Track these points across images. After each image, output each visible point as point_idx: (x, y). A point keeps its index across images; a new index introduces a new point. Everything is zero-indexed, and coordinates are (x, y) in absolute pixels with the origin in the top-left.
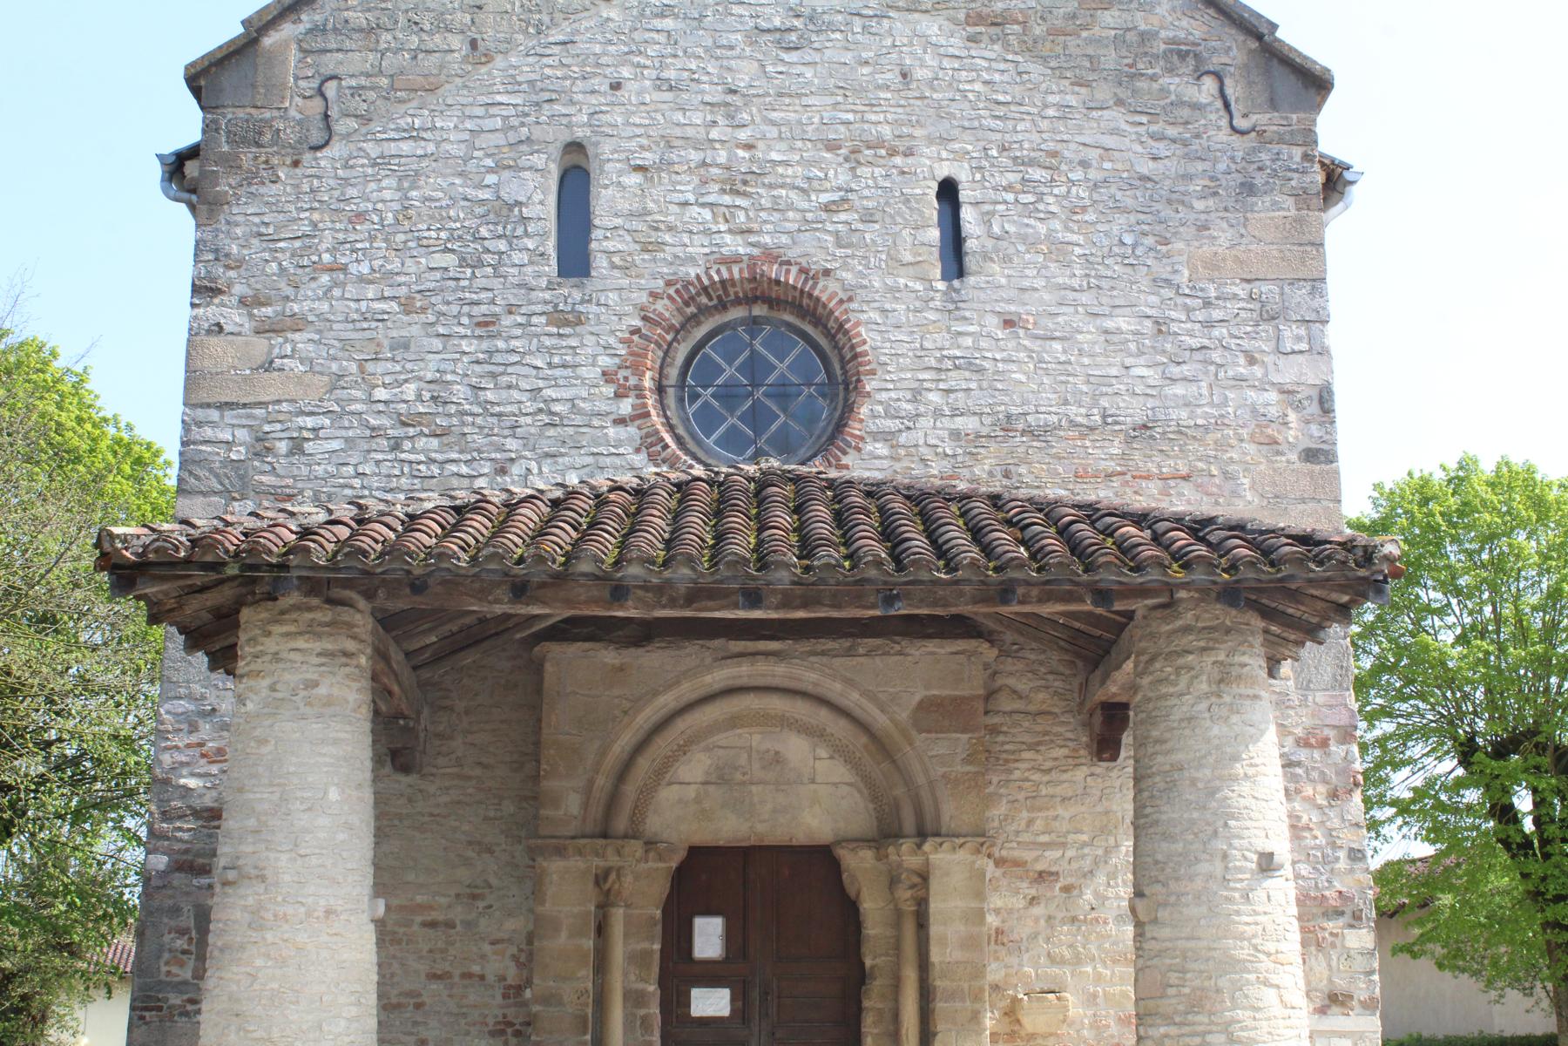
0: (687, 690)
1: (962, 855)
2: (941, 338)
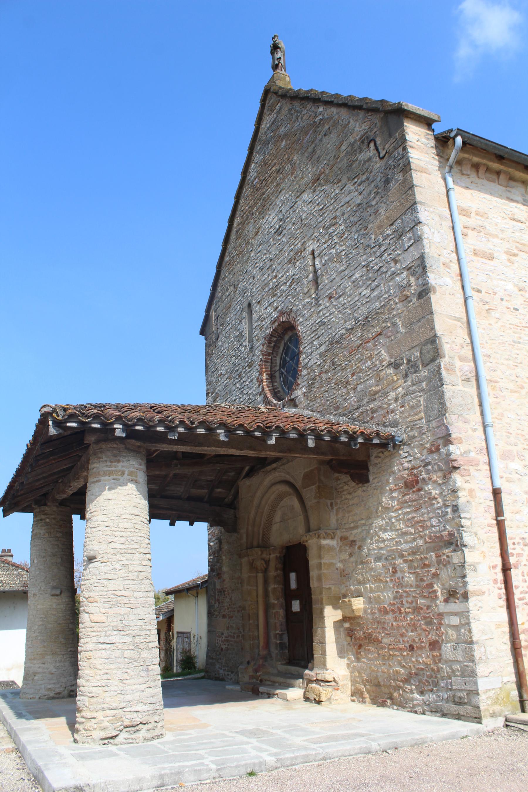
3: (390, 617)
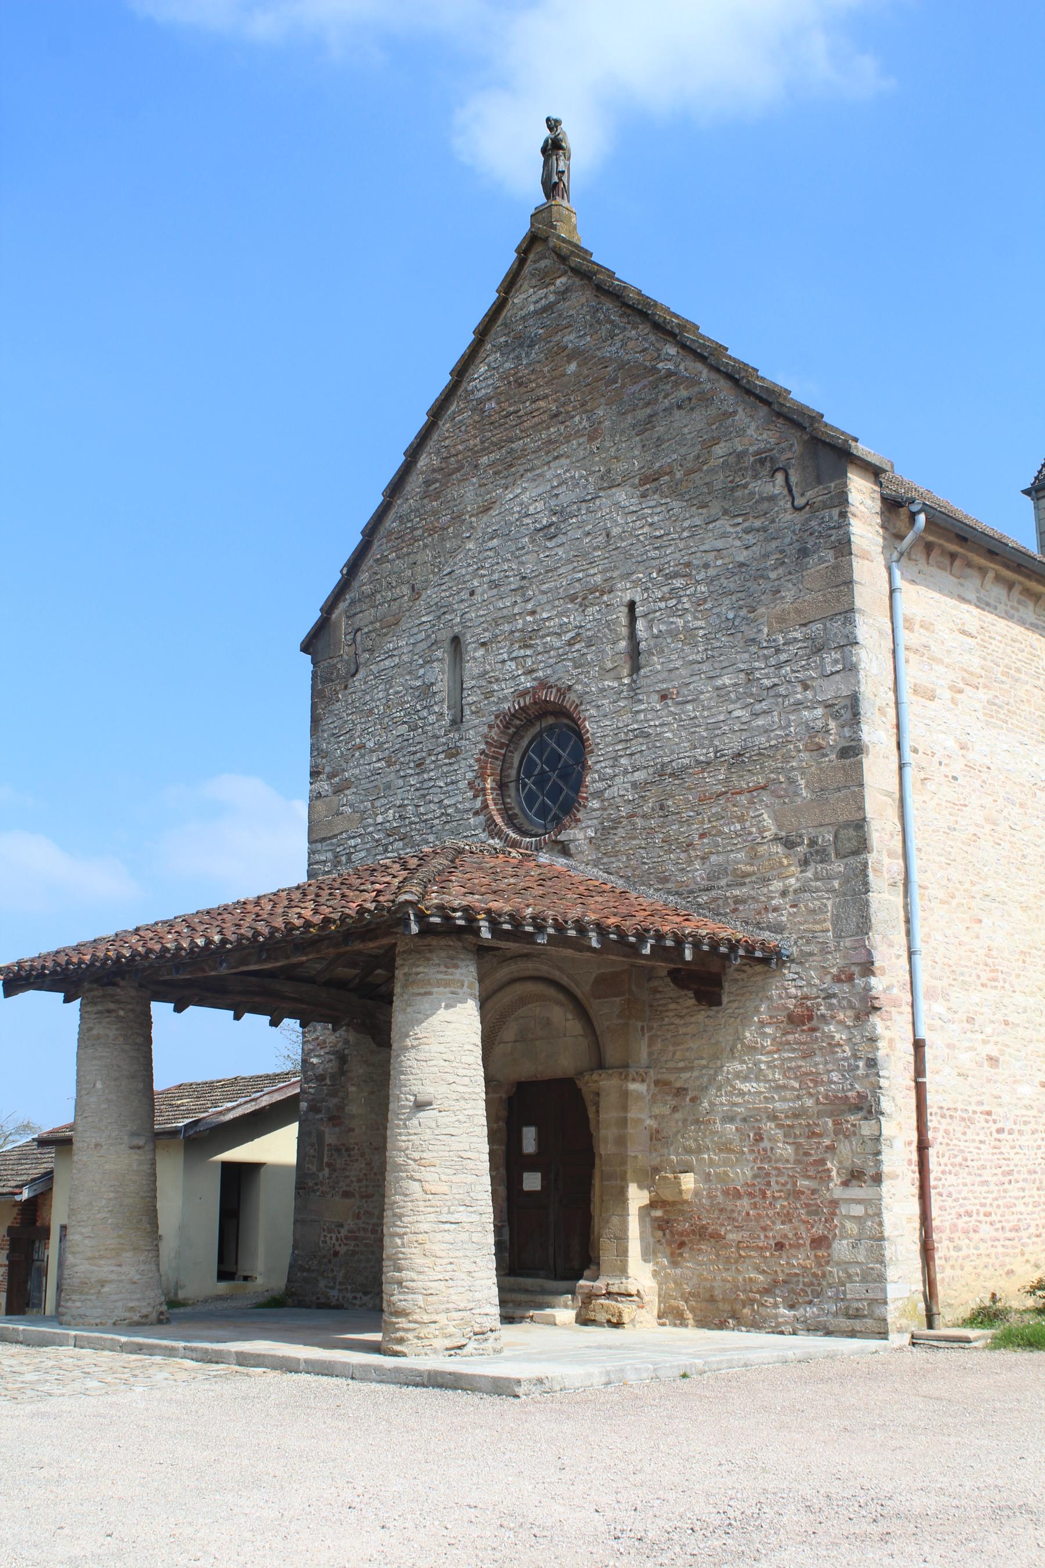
1: (615, 1082)
2: (627, 718)
3: (745, 1202)
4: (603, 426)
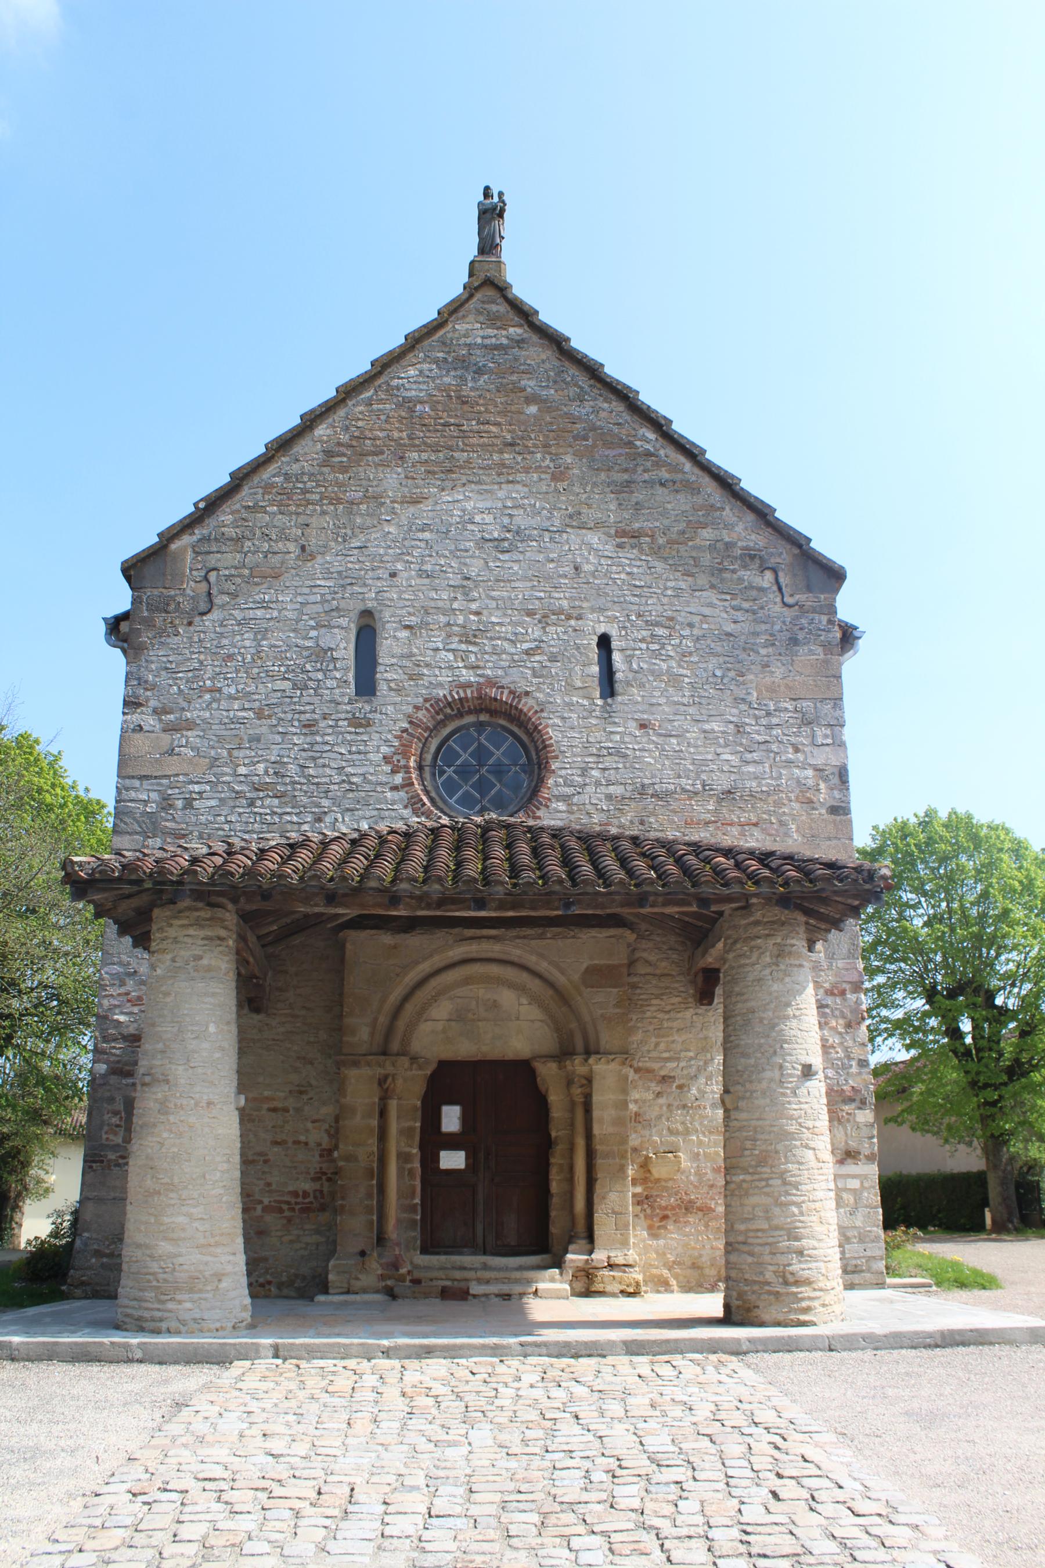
0: (437, 961)
1: (613, 1066)
2: (599, 735)
4: (571, 472)
